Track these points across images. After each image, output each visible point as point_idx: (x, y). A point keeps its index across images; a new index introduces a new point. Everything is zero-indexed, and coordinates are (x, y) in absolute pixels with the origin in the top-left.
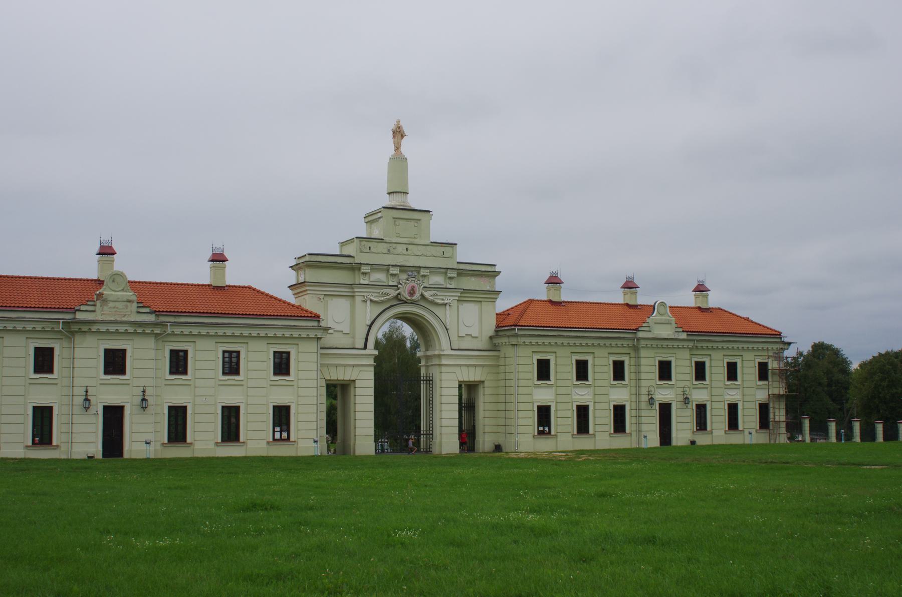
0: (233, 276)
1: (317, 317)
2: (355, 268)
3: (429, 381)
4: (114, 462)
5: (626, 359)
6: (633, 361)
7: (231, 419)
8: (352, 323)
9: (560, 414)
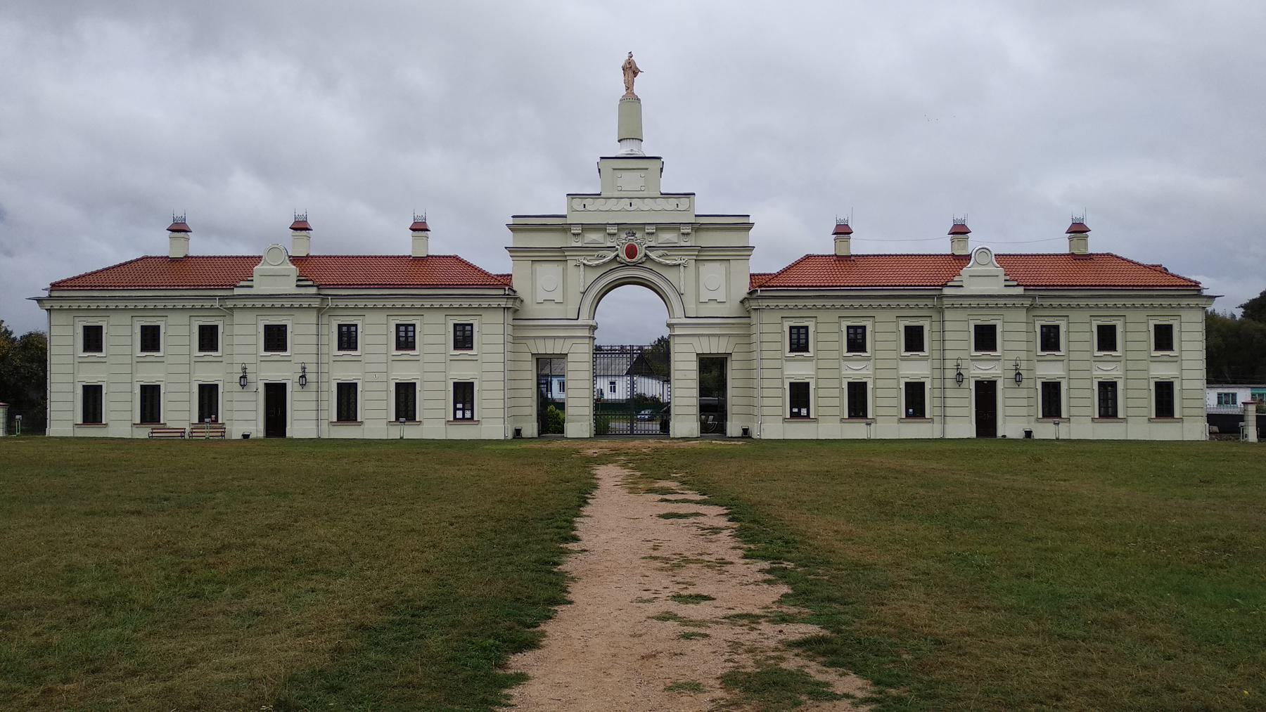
0: (437, 245)
2: (565, 229)
5: (926, 324)
6: (936, 326)
7: (406, 398)
9: (821, 393)
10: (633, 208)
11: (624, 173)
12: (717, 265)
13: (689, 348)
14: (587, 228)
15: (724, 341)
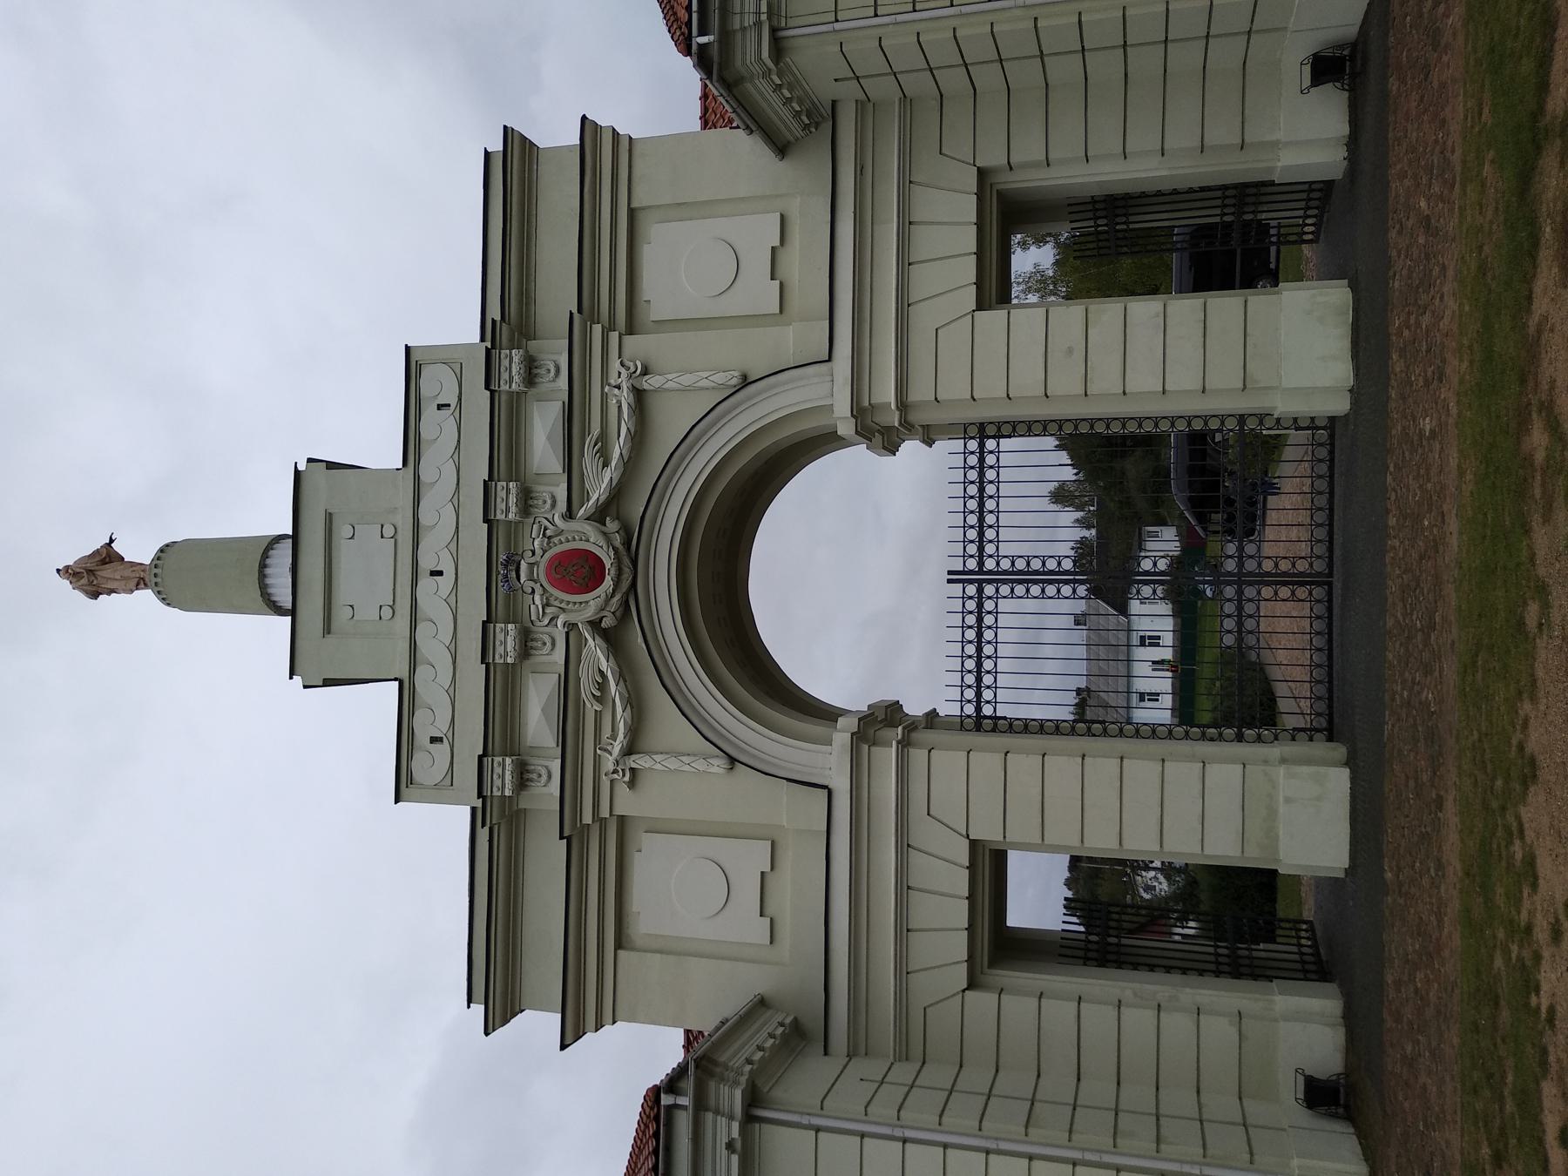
10: (447, 566)
11: (343, 595)
12: (650, 256)
13: (955, 341)
14: (501, 729)
15: (928, 204)
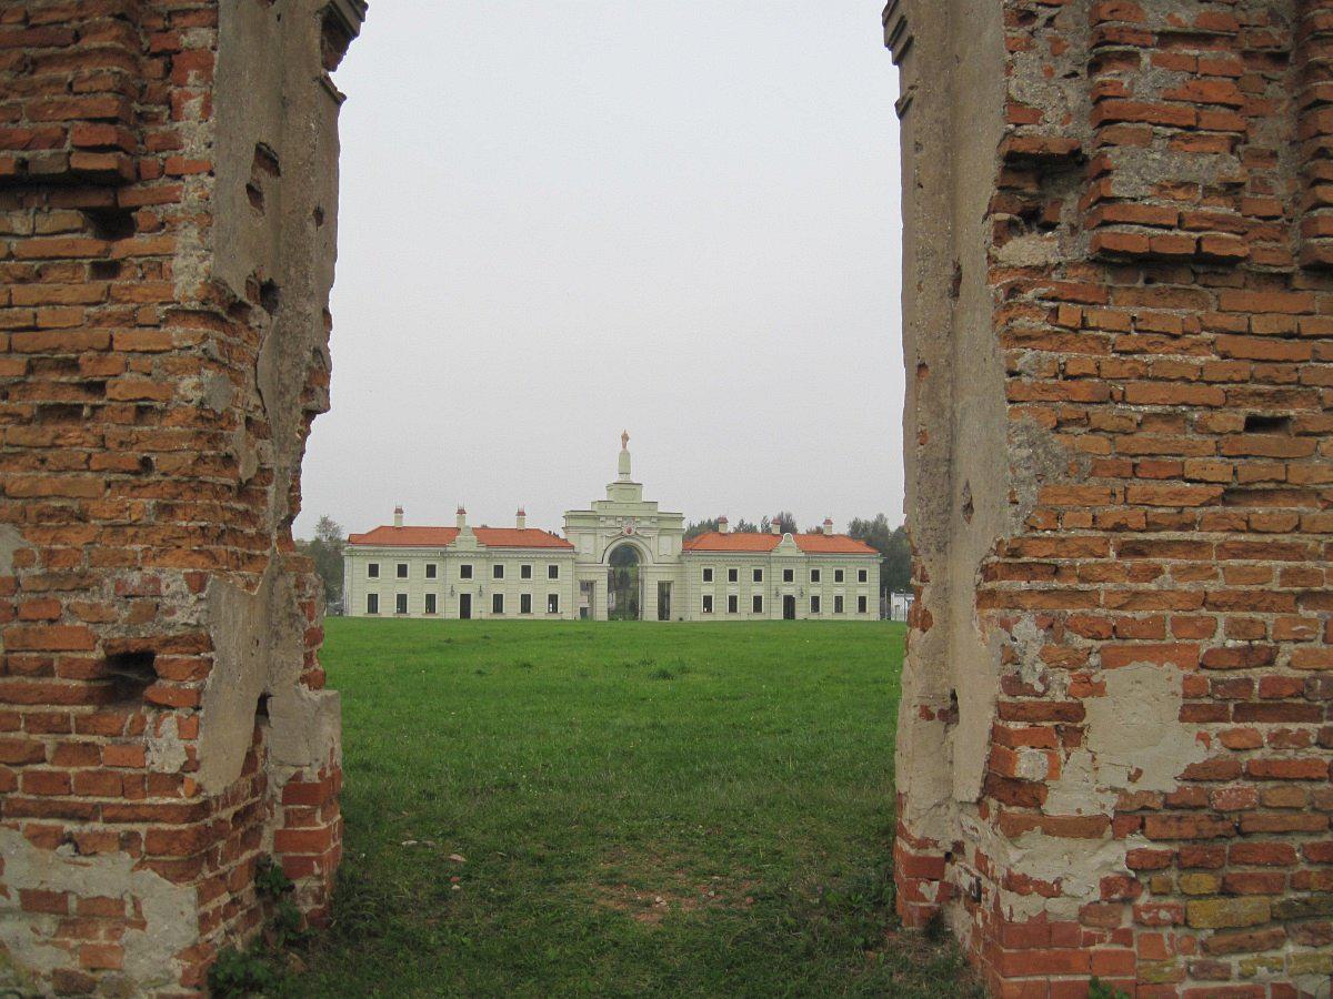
0: (529, 524)
1: (573, 547)
2: (597, 518)
3: (642, 581)
4: (465, 621)
8: (594, 549)
